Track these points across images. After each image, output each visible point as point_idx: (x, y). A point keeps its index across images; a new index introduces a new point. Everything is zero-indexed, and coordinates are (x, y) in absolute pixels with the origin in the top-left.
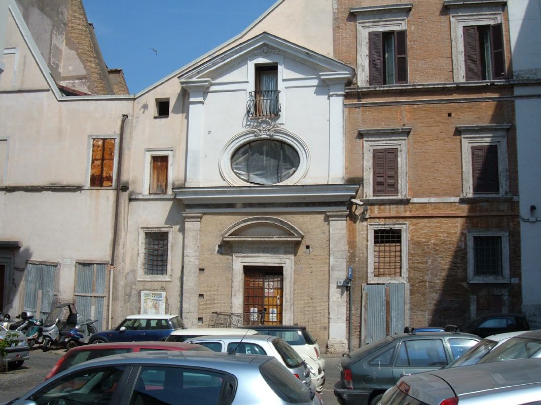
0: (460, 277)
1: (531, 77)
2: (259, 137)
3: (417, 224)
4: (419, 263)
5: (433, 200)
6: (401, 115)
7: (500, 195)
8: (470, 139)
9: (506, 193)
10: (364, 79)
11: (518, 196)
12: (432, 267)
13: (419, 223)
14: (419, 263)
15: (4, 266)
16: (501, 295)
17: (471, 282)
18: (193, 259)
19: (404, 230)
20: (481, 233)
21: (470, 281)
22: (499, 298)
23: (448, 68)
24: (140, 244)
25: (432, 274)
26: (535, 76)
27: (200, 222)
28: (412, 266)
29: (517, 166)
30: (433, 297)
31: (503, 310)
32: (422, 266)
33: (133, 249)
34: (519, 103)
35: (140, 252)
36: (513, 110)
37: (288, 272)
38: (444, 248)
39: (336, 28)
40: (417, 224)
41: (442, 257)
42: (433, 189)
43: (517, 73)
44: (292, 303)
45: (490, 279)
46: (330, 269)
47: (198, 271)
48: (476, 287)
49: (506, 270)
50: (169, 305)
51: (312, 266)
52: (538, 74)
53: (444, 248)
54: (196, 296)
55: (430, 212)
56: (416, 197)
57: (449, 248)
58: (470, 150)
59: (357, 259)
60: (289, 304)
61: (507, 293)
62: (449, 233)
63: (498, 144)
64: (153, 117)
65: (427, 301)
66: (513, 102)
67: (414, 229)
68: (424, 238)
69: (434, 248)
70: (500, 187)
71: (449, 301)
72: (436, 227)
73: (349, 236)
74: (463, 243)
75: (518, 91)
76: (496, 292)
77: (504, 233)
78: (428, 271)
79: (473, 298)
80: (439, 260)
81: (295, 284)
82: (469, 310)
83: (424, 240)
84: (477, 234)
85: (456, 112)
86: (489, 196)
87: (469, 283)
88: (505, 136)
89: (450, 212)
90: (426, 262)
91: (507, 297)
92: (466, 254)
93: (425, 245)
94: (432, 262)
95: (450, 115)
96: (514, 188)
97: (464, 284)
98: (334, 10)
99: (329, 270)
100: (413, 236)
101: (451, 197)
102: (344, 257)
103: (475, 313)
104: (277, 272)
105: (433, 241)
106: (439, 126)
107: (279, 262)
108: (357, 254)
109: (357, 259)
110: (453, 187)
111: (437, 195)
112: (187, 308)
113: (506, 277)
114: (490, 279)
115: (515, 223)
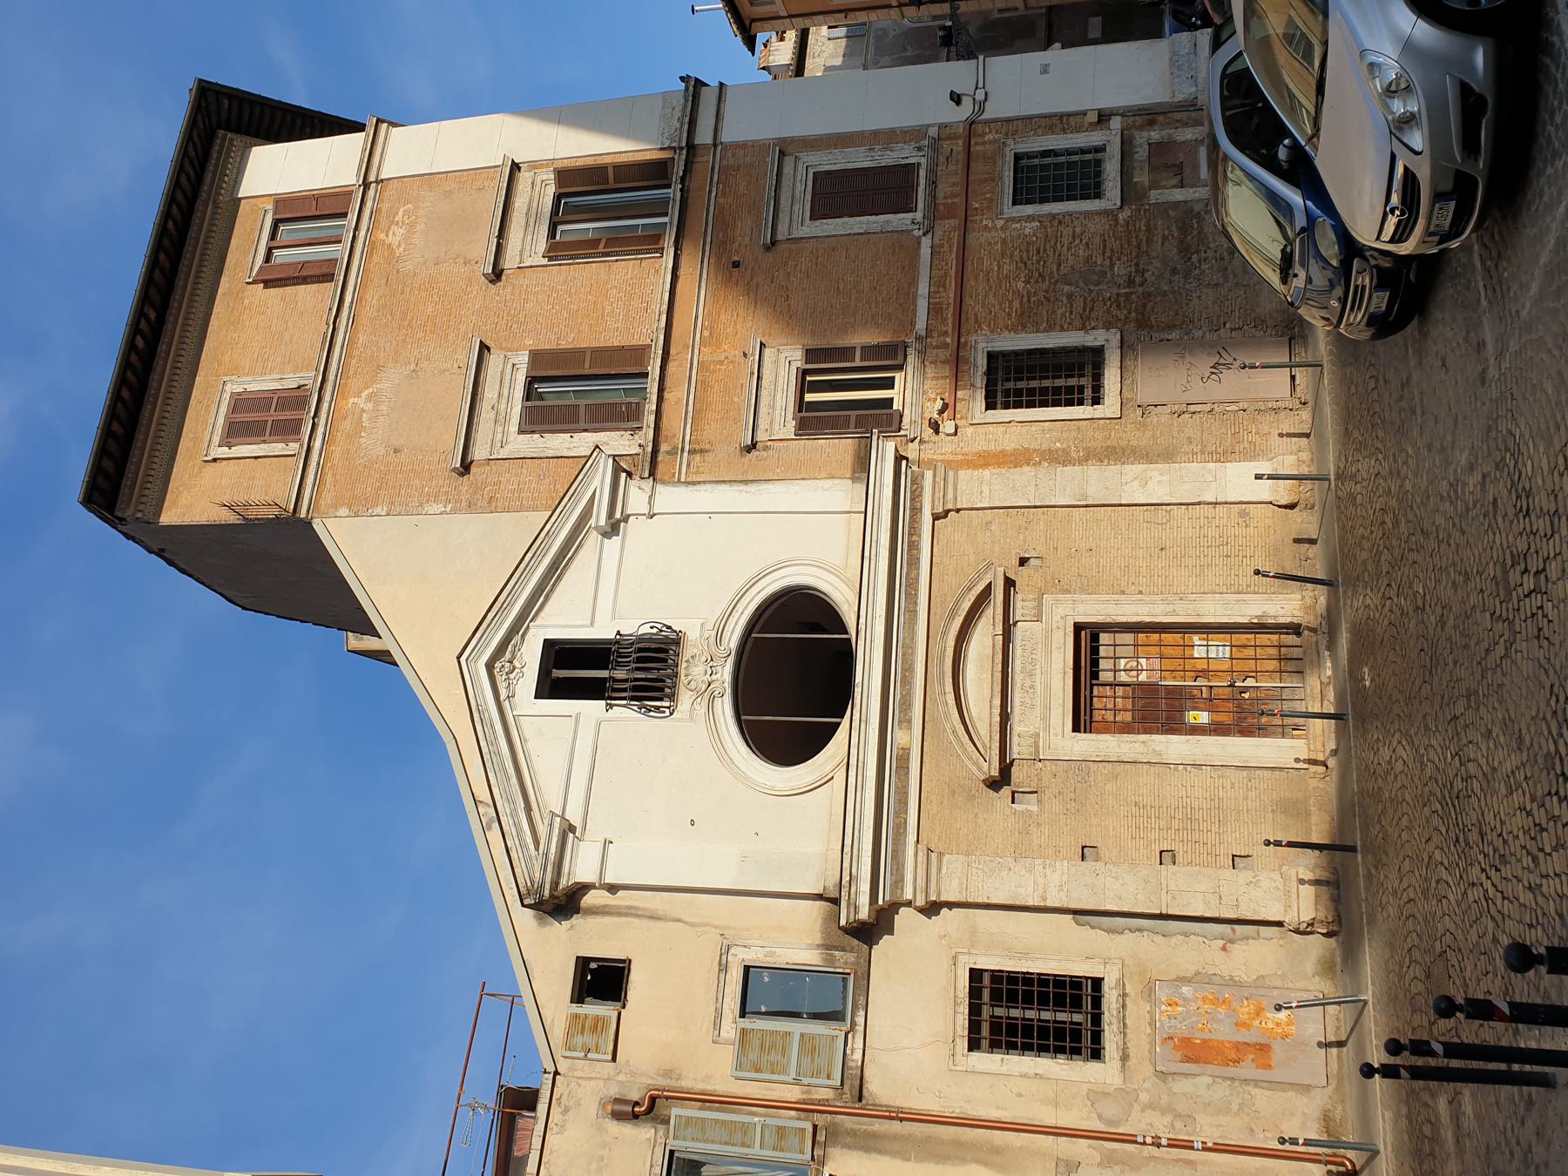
0: (1107, 227)
1: (678, 114)
2: (726, 685)
3: (976, 321)
4: (1071, 312)
5: (923, 289)
6: (721, 363)
7: (923, 161)
8: (795, 224)
9: (919, 149)
10: (627, 443)
11: (928, 126)
12: (1081, 283)
13: (976, 315)
14: (1071, 312)
15: (893, 388)
16: (1149, 144)
17: (1119, 204)
18: (1055, 878)
19: (990, 345)
20: (1006, 192)
21: (1115, 204)
22: (1156, 148)
23: (633, 270)
24: (1004, 1069)
25: (1098, 283)
26: (677, 110)
27: (941, 855)
28: (1078, 323)
29: (863, 132)
30: (1154, 278)
31: (1183, 139)
32: (1078, 304)
33: (1020, 1095)
34: (727, 136)
35: (1032, 1072)
36: (743, 145)
37: (1093, 610)
38: (1038, 262)
39: (492, 505)
40: (976, 321)
41: (1059, 265)
42: (898, 290)
43: (665, 140)
44: (1177, 597)
45: (1112, 168)
46: (1084, 503)
47: (1088, 864)
48: (1130, 192)
49: (1094, 138)
50: (1198, 973)
51: (1073, 550)
52: (674, 104)
53: (1038, 262)
54: (1168, 870)
55: (952, 295)
56: (913, 324)
57: (1038, 252)
58: (818, 223)
59: (1058, 445)
60: (1179, 606)
61: (1145, 134)
62: (1003, 255)
63: (811, 171)
64: (637, 984)
65: (1165, 288)
66: (726, 147)
67: (989, 326)
68: (1011, 303)
69: (1037, 282)
70: (906, 161)
71: (1163, 244)
72: (988, 280)
73: (999, 465)
74: (1027, 224)
75: (704, 136)
76: (1142, 153)
77: (1007, 149)
78: (1091, 291)
79: (1155, 196)
80: (1063, 270)
81: (1123, 593)
82: (1186, 202)
83: (1016, 304)
84: (1008, 199)
85: (730, 252)
86: (922, 181)
87: (1121, 207)
88: (796, 157)
89: (954, 255)
90: (1070, 296)
91: (1152, 134)
92: (1053, 216)
93: (1029, 302)
94: (1070, 284)
95: (736, 265)
96: (912, 135)
97: (1122, 216)
98: (448, 510)
99: (1087, 506)
100: (1007, 328)
101: (919, 255)
102: (1053, 471)
103: (1191, 190)
104: (1087, 638)
105: (1020, 285)
106: (757, 285)
107: (1061, 633)
108: (1045, 447)
109: (1058, 445)
110: (897, 250)
111: (914, 282)
112: (1207, 903)
113: (1110, 138)
114: (1112, 168)
115: (987, 130)
